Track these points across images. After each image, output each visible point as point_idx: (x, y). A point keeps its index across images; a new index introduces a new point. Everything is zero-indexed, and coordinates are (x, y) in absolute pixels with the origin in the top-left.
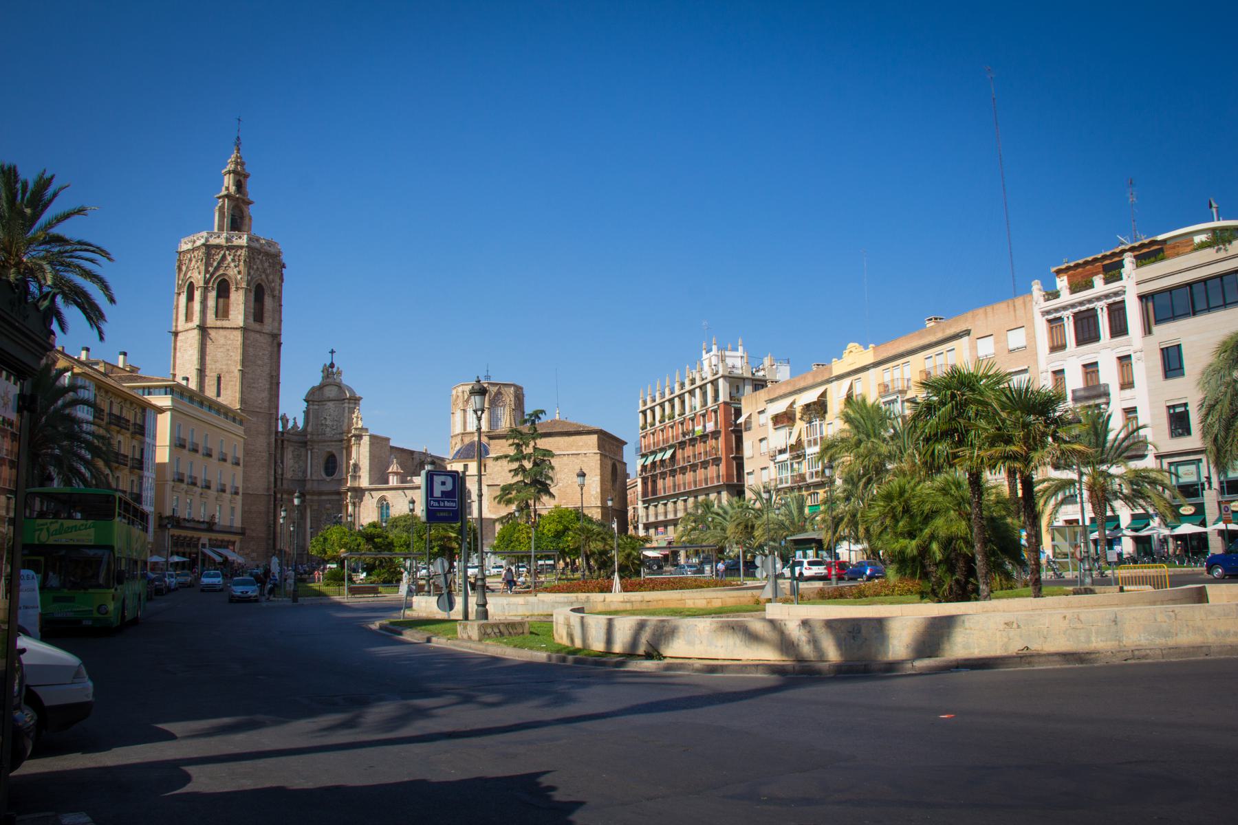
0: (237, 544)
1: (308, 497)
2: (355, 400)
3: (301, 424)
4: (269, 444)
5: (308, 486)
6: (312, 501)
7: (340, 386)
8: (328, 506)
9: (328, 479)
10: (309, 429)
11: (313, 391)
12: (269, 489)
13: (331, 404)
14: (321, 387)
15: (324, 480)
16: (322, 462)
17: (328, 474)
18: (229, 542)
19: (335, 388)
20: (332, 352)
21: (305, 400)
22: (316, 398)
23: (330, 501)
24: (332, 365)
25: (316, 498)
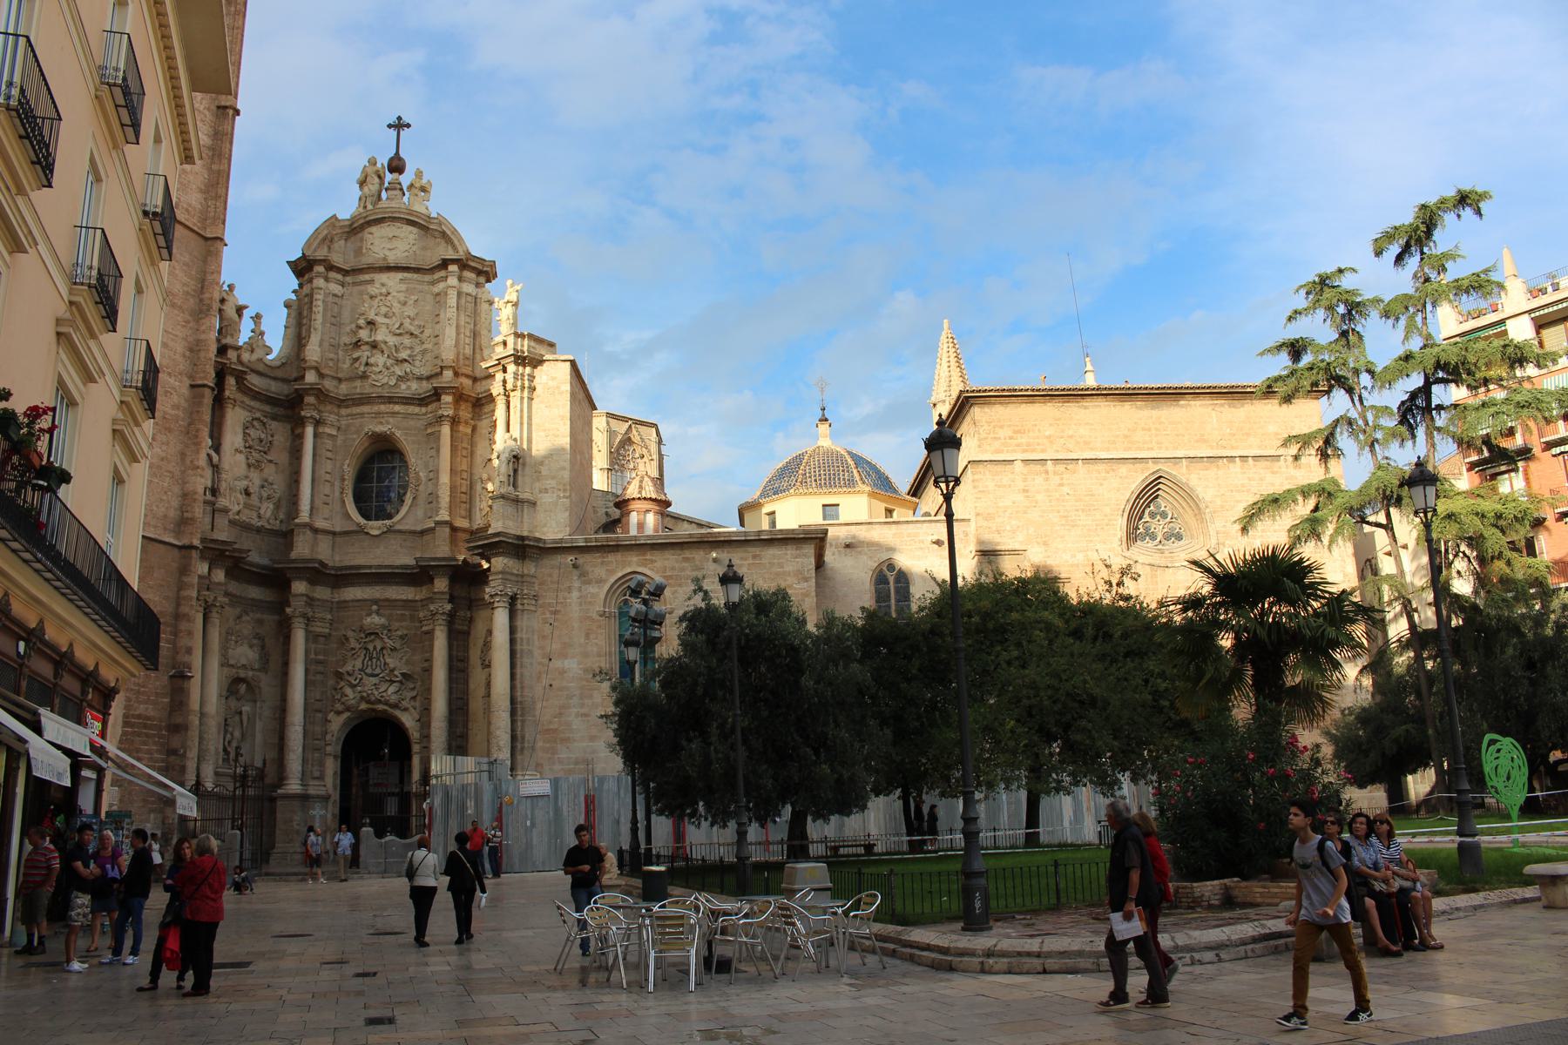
0: (117, 708)
1: (299, 587)
2: (485, 272)
3: (276, 341)
4: (195, 348)
5: (302, 548)
6: (311, 601)
7: (428, 228)
8: (374, 620)
9: (375, 527)
10: (313, 352)
11: (333, 232)
12: (183, 523)
13: (392, 281)
14: (356, 228)
15: (361, 531)
16: (349, 470)
17: (367, 517)
18: (89, 678)
19: (409, 233)
20: (399, 125)
21: (302, 268)
22: (337, 259)
23: (382, 604)
24: (397, 166)
25: (322, 593)
